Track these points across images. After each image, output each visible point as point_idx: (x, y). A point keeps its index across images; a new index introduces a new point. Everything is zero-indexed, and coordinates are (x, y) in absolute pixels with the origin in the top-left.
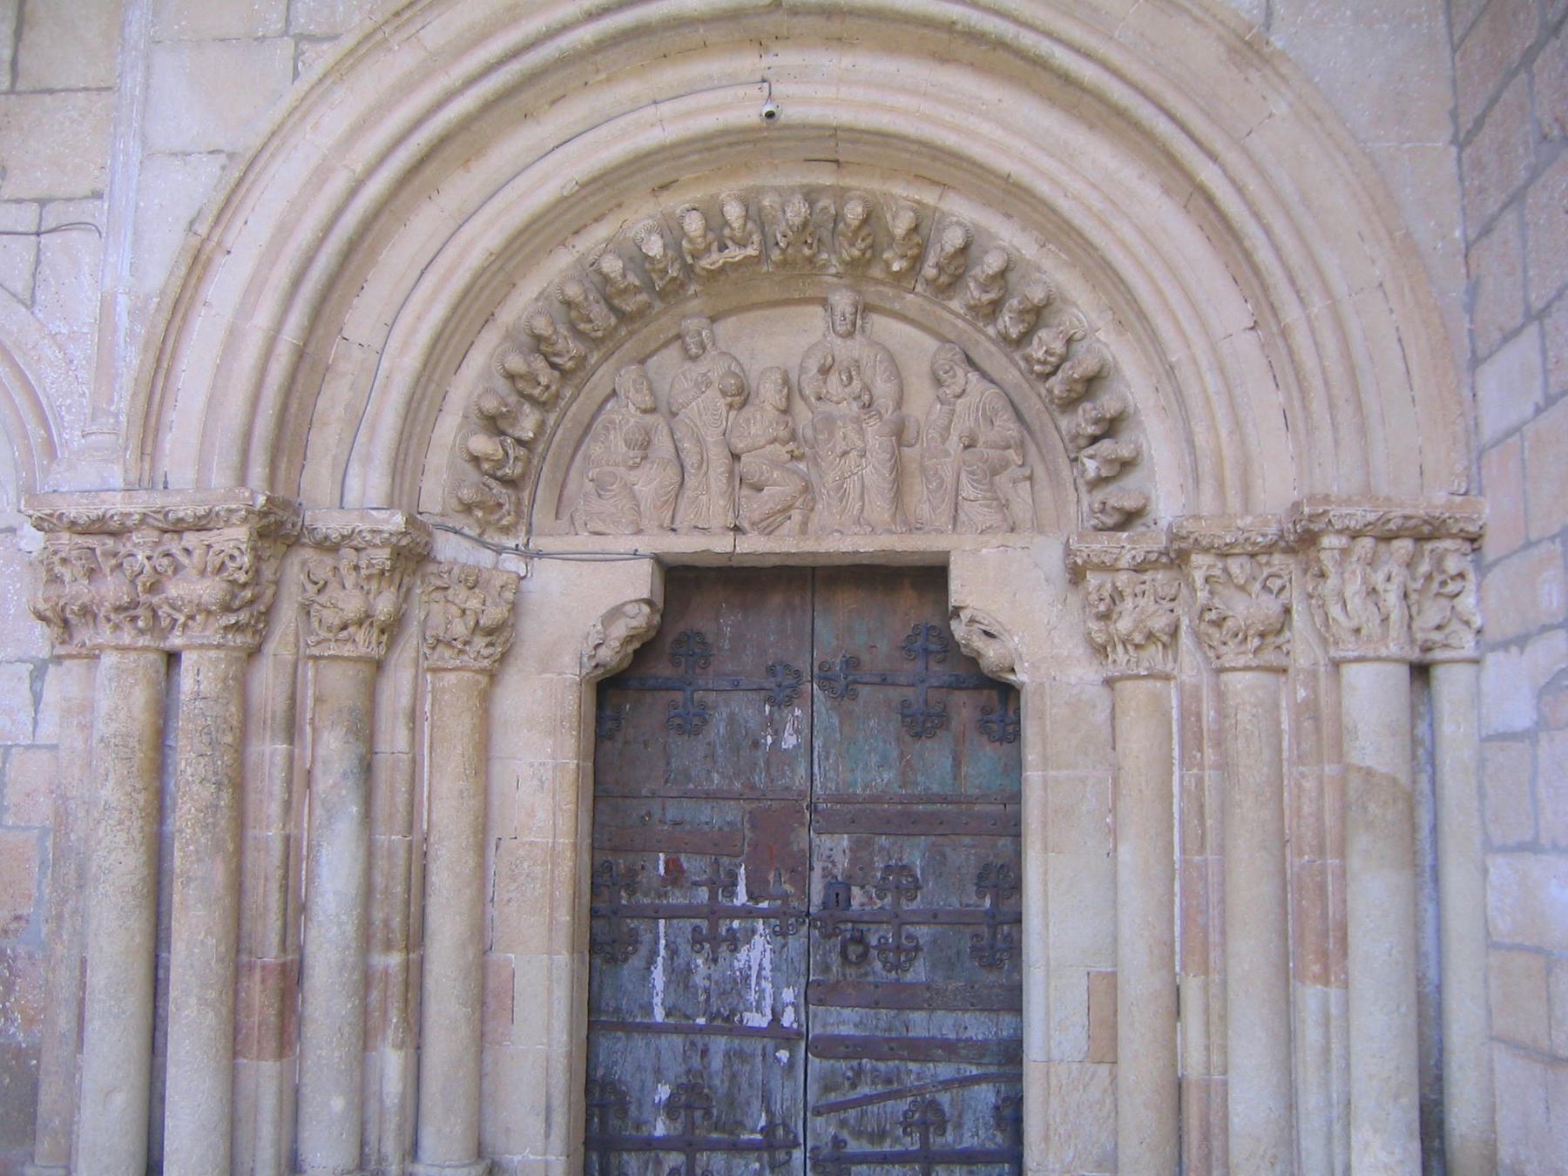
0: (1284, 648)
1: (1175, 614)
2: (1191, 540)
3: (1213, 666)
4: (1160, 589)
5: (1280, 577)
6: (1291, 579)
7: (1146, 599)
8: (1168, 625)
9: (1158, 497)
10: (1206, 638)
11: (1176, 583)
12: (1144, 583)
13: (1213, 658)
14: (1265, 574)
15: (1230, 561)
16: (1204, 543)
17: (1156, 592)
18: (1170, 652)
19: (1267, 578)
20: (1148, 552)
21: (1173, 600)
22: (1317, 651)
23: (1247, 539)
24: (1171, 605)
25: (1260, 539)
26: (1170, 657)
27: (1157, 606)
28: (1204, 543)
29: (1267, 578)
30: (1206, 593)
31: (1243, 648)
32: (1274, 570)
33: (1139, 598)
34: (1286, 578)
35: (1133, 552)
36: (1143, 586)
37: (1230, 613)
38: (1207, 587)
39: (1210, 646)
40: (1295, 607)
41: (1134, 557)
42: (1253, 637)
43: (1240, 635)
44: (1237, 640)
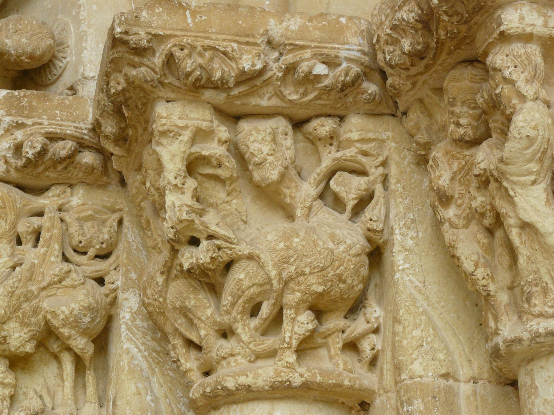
0: (366, 346)
1: (108, 286)
2: (158, 60)
3: (195, 393)
4: (74, 229)
5: (362, 173)
6: (385, 179)
7: (41, 250)
8: (89, 308)
9: (81, 38)
10: (181, 324)
11: (116, 216)
12: (40, 214)
13: (196, 376)
14: (327, 162)
15: (245, 126)
16: (188, 65)
17: (65, 233)
18: (90, 377)
19: (331, 174)
20: (52, 138)
21: (103, 256)
22: (453, 345)
23: (291, 69)
24: (101, 266)
25: (320, 69)
26: (91, 390)
27: (66, 266)
28: (188, 65)
29: (331, 174)
30: (187, 199)
31: (270, 342)
32: (349, 153)
33: (27, 246)
34: (376, 173)
35: (19, 135)
36: (36, 221)
37: (244, 249)
38: (191, 183)
39: (190, 344)
40: (397, 237)
41: (18, 148)
42: (298, 310)
43: (265, 310)
44: (255, 322)
